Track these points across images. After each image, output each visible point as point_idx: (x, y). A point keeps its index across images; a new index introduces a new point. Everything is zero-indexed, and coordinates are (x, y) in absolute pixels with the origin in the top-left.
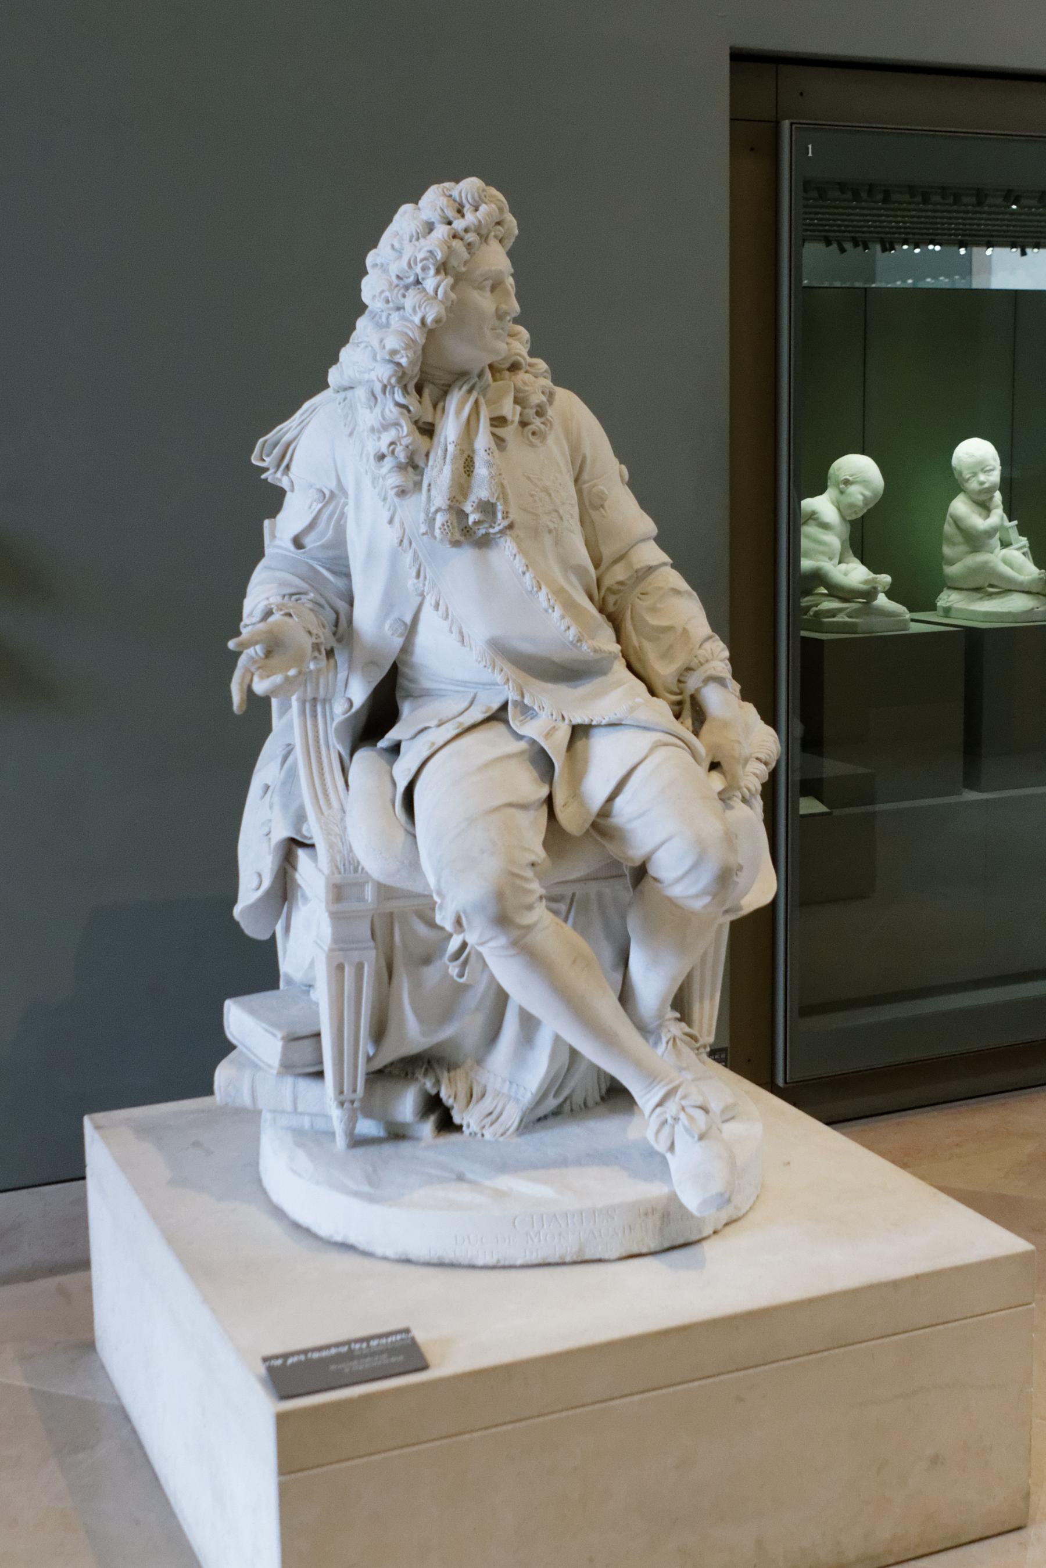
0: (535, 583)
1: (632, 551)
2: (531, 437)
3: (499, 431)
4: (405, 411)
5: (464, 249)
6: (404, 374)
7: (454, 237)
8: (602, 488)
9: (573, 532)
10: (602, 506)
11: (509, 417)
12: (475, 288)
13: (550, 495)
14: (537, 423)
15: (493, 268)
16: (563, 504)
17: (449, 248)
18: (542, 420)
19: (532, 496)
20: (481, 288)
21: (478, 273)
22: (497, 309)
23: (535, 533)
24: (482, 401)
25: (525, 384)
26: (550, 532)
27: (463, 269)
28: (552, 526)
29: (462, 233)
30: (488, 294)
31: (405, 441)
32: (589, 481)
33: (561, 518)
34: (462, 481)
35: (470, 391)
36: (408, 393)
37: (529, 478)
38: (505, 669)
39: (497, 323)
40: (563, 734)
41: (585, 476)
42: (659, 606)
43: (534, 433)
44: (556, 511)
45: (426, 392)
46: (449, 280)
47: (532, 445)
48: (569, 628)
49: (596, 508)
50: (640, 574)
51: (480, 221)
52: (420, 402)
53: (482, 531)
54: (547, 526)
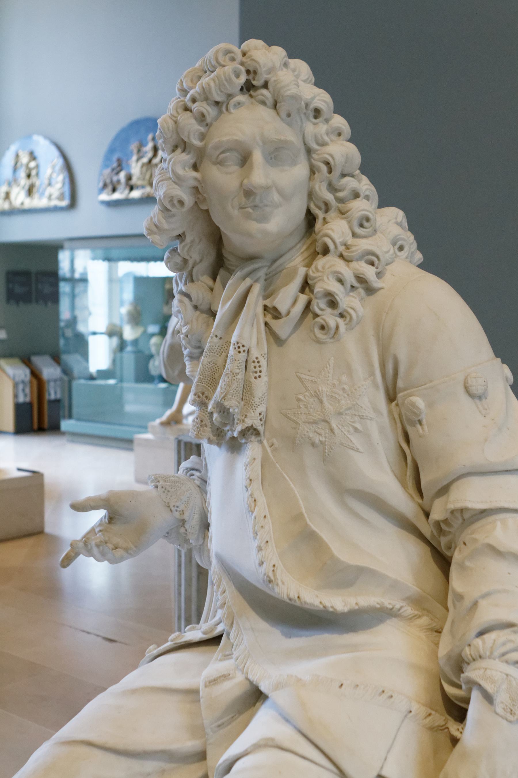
0: (251, 500)
1: (455, 485)
2: (317, 331)
3: (273, 323)
4: (186, 300)
5: (193, 121)
6: (185, 261)
7: (187, 109)
8: (413, 399)
9: (357, 450)
10: (420, 422)
11: (283, 308)
12: (215, 164)
13: (321, 402)
14: (330, 318)
15: (224, 139)
16: (340, 414)
17: (176, 122)
18: (337, 312)
19: (299, 400)
20: (220, 163)
21: (210, 146)
22: (241, 184)
23: (293, 443)
24: (257, 289)
25: (317, 270)
26: (313, 445)
27: (197, 143)
28: (317, 439)
29: (190, 104)
30: (235, 168)
31: (184, 330)
32: (405, 390)
33: (332, 430)
34: (217, 376)
35: (244, 278)
36: (192, 281)
37: (300, 379)
38: (227, 591)
39: (244, 200)
40: (233, 688)
41: (400, 384)
42: (468, 564)
43: (322, 328)
44: (326, 421)
45: (218, 279)
46: (187, 158)
47: (318, 341)
48: (263, 563)
49: (413, 424)
50: (466, 516)
51: (203, 88)
52: (212, 290)
53: (229, 434)
54: (309, 438)
